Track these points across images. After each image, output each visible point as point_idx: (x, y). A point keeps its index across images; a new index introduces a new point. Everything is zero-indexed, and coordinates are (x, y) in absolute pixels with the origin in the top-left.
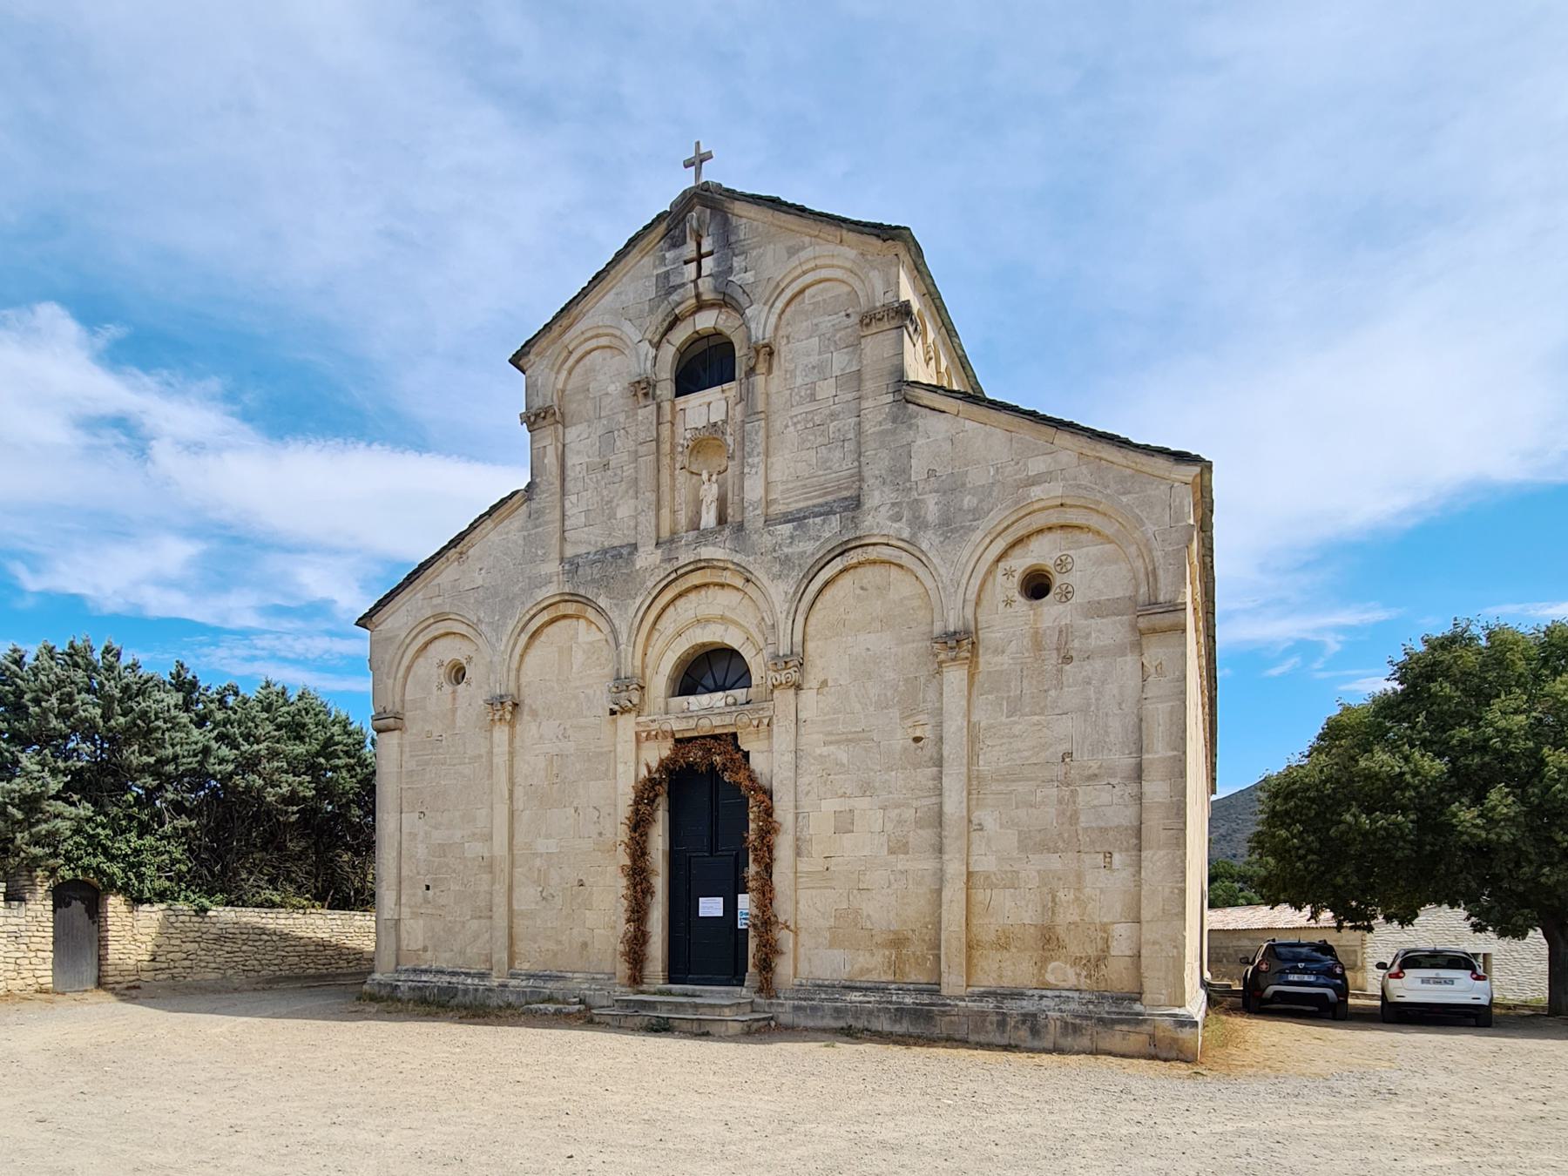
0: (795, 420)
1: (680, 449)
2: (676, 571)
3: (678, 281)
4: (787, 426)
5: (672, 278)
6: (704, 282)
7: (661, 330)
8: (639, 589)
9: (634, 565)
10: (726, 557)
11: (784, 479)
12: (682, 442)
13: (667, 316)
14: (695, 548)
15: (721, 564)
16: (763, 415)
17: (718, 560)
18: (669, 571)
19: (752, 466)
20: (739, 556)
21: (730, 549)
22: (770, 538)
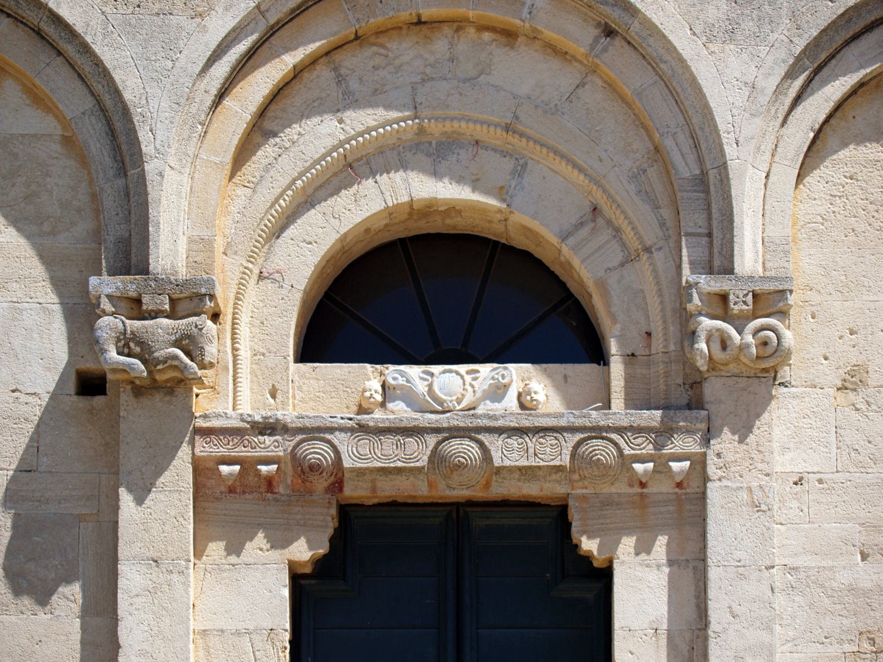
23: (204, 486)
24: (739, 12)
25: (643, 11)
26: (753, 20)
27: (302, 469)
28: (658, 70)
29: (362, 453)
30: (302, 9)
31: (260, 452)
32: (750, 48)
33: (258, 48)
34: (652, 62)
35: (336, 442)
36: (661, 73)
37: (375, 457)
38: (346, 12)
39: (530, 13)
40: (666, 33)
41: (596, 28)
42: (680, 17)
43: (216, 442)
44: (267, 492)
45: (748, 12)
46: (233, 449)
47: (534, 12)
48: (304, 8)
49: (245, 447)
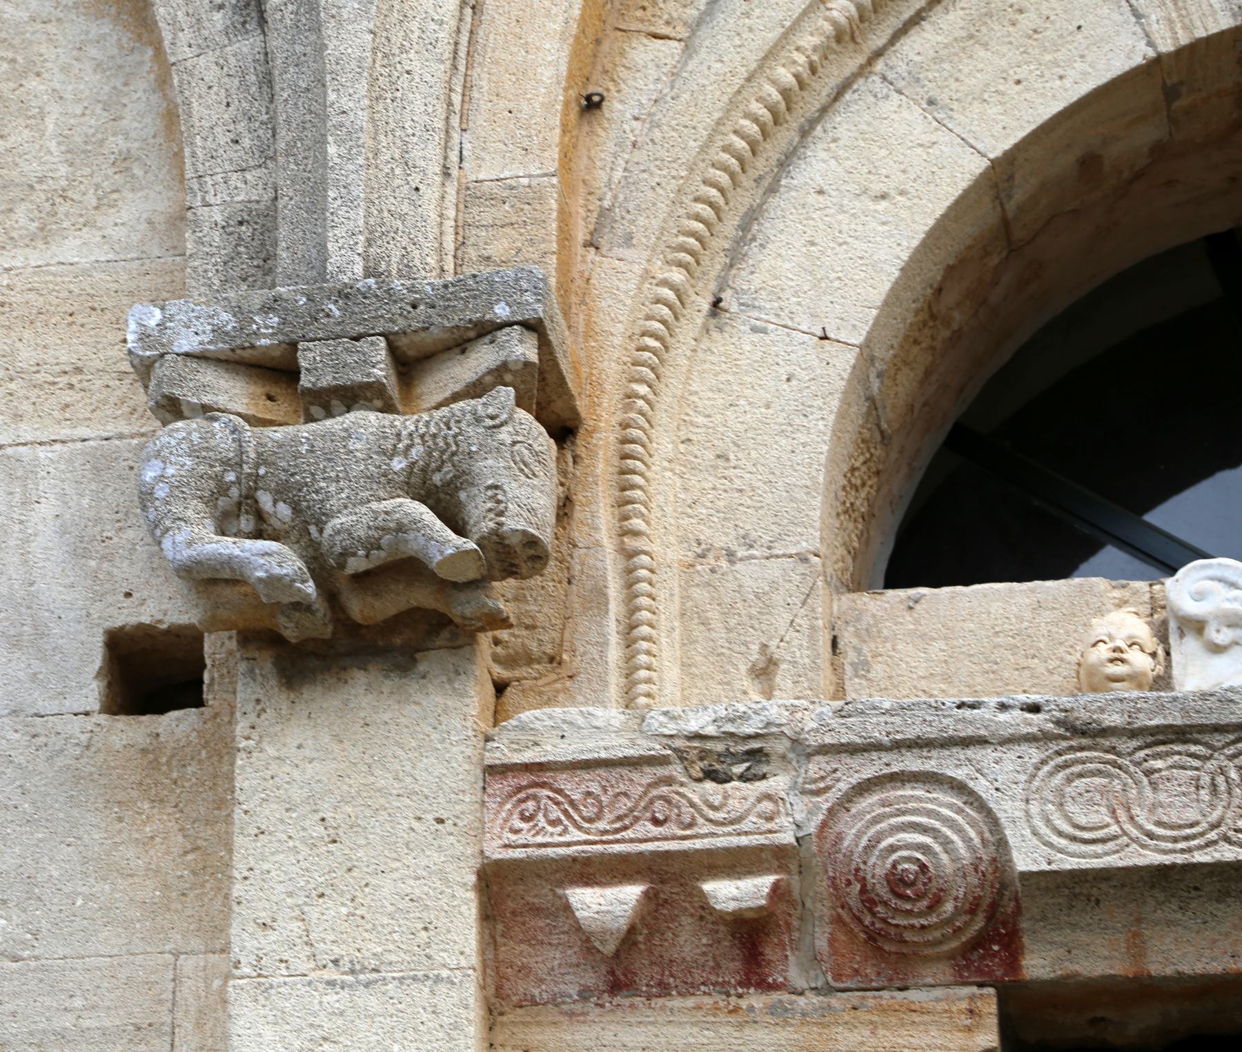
23: (525, 970)
27: (863, 890)
29: (1082, 820)
31: (713, 835)
35: (981, 787)
37: (1135, 832)
43: (556, 813)
44: (745, 983)
46: (617, 831)
49: (656, 822)
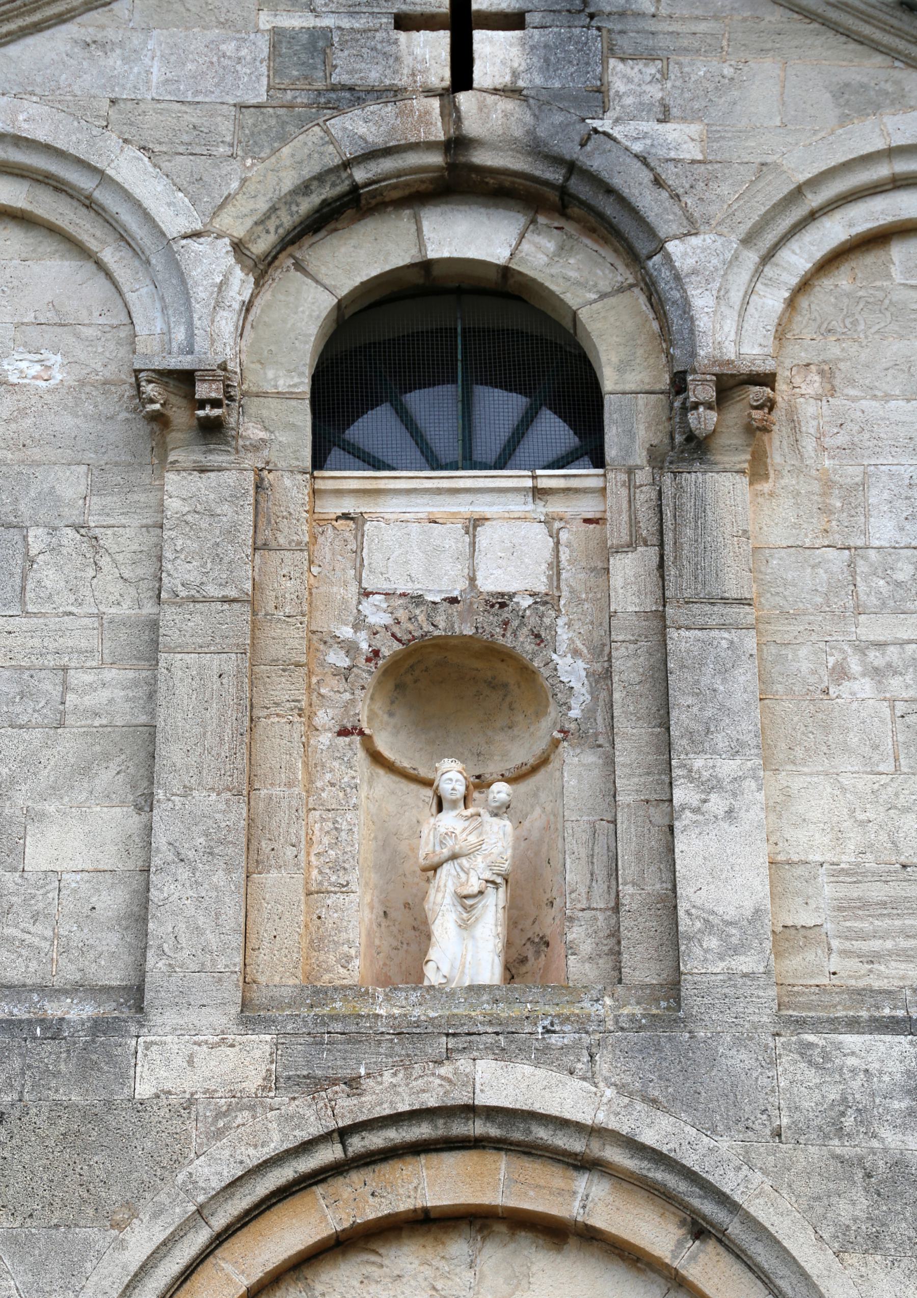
0: (875, 657)
1: (338, 658)
2: (344, 1134)
3: (374, 75)
4: (841, 673)
5: (340, 58)
6: (482, 107)
7: (287, 220)
8: (145, 1187)
9: (124, 1076)
10: (602, 1118)
11: (847, 859)
12: (346, 632)
13: (320, 178)
14: (449, 1053)
15: (576, 1145)
16: (747, 615)
17: (562, 1123)
18: (314, 1130)
19: (710, 786)
20: (665, 1122)
21: (621, 1089)
22: (812, 1076)
24: (885, 1208)
25: (745, 1206)
26: (906, 1219)
28: (772, 1287)
30: (262, 1209)
32: (906, 1261)
33: (198, 1265)
34: (763, 1277)
36: (776, 1291)
38: (323, 1211)
39: (584, 1207)
40: (779, 1237)
41: (680, 1228)
42: (798, 1216)
45: (899, 1207)
47: (590, 1205)
48: (264, 1207)
